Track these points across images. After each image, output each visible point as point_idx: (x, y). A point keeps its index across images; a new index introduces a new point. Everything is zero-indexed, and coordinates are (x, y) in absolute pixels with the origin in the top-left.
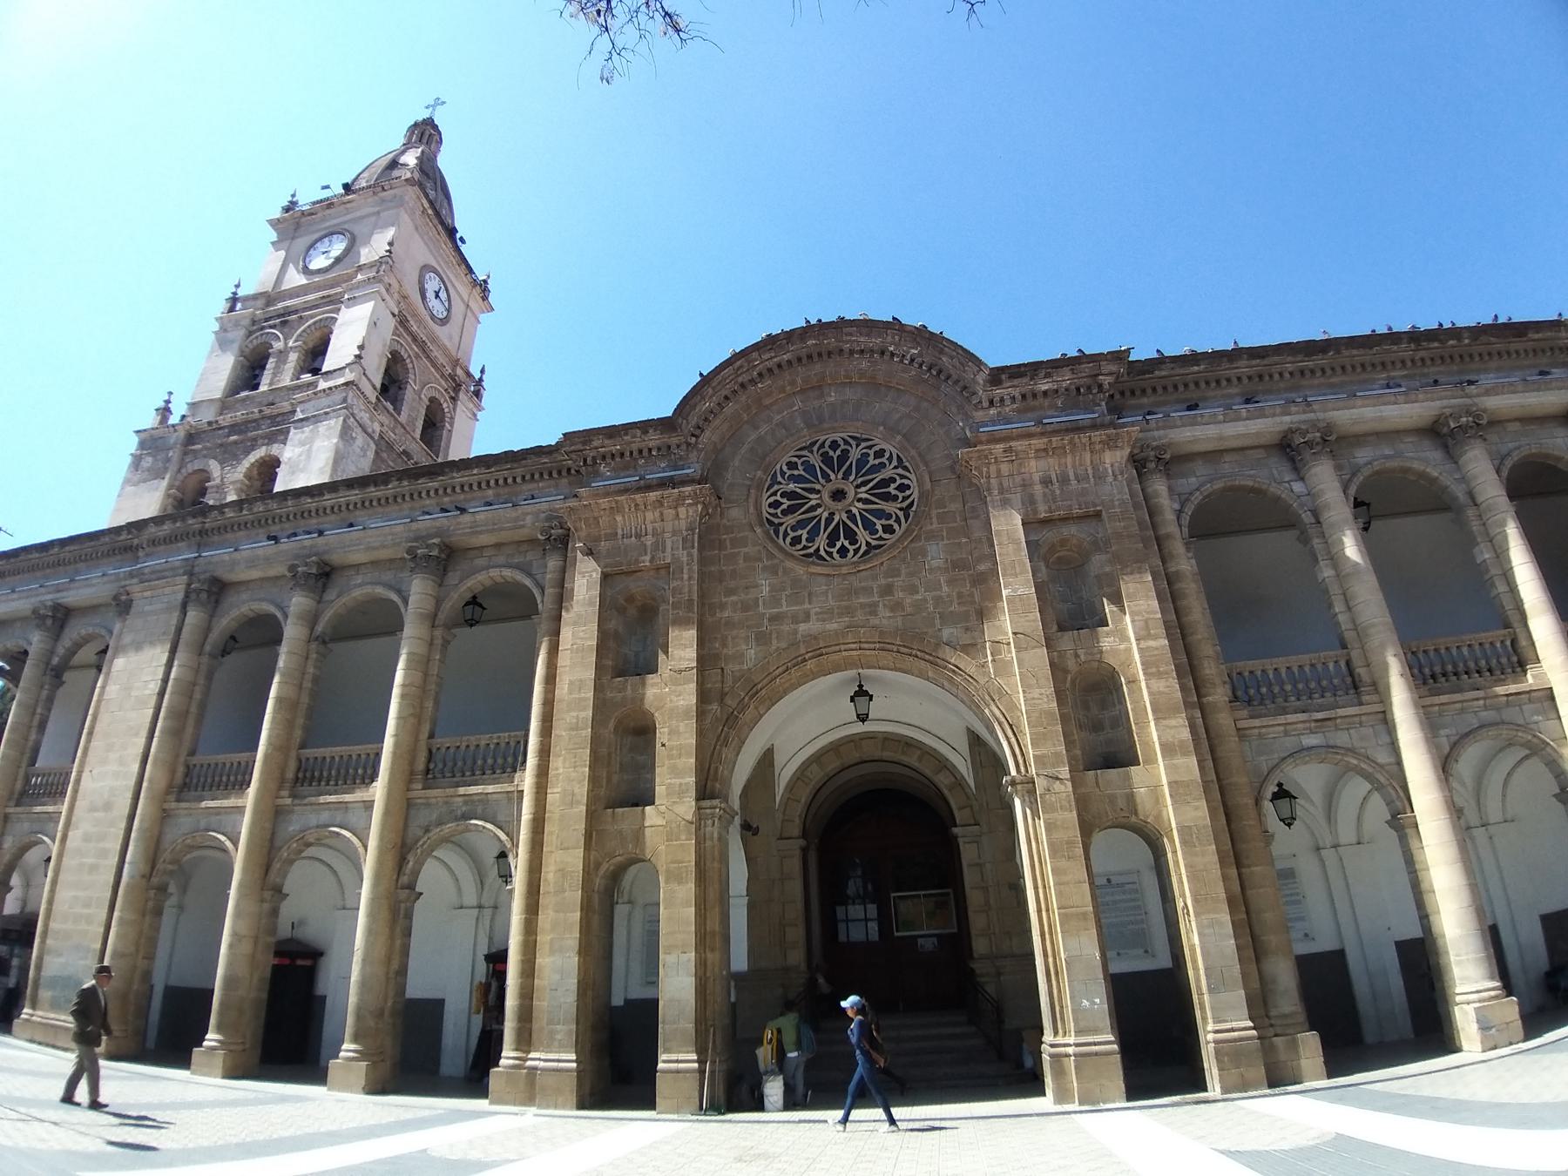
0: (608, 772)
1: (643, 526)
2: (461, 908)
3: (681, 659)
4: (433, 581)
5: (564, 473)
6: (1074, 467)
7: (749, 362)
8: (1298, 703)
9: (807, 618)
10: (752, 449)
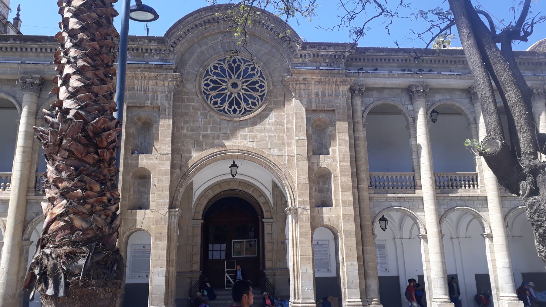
1: (147, 87)
3: (164, 150)
6: (328, 90)
7: (200, 16)
8: (393, 190)
9: (218, 138)
10: (198, 56)
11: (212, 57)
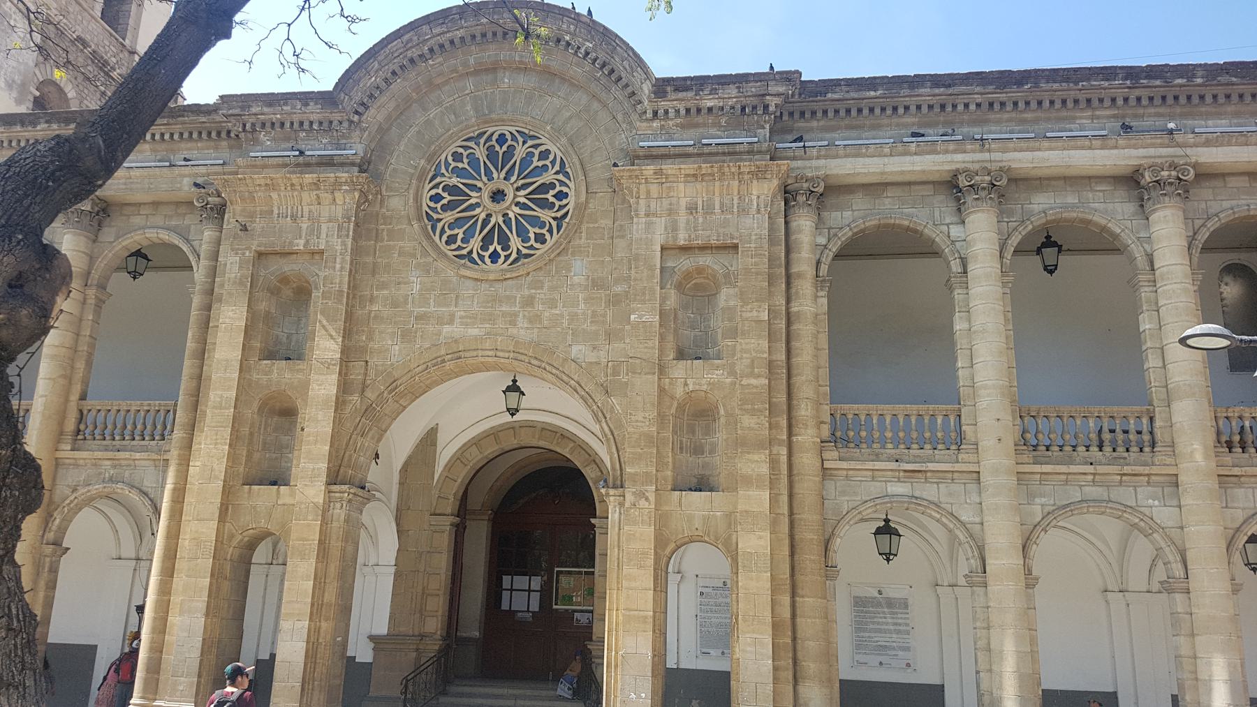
0: (248, 451)
1: (300, 208)
2: (120, 559)
4: (86, 237)
5: (224, 135)
9: (451, 322)
10: (419, 132)
11: (450, 133)
